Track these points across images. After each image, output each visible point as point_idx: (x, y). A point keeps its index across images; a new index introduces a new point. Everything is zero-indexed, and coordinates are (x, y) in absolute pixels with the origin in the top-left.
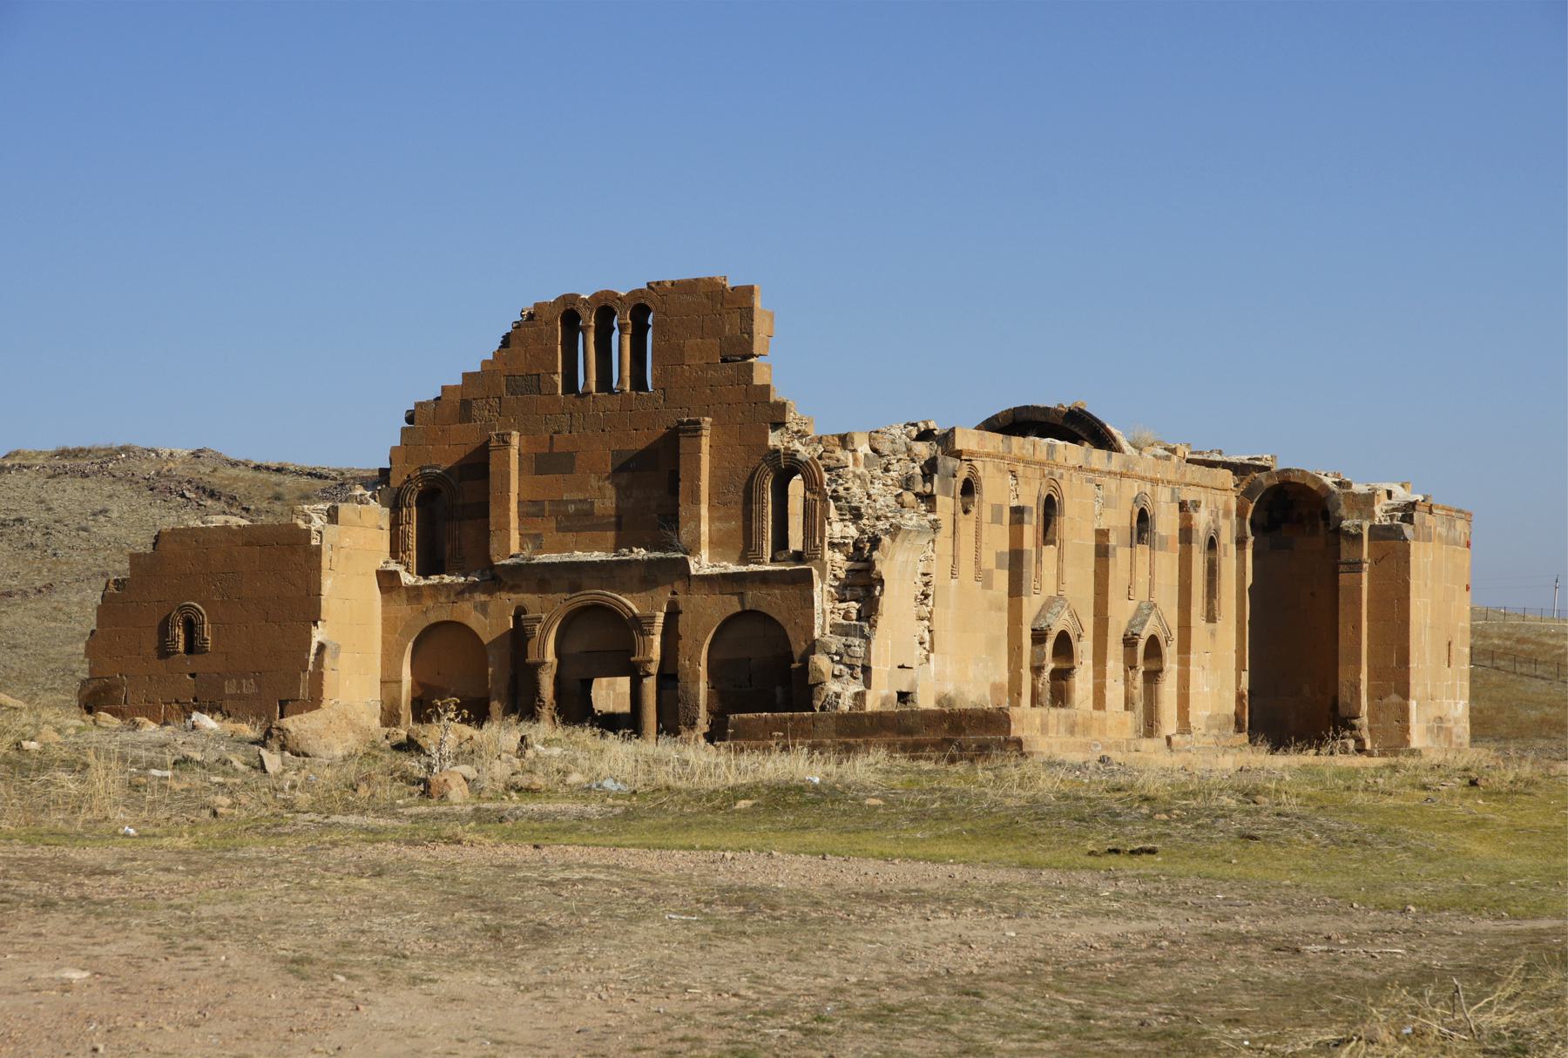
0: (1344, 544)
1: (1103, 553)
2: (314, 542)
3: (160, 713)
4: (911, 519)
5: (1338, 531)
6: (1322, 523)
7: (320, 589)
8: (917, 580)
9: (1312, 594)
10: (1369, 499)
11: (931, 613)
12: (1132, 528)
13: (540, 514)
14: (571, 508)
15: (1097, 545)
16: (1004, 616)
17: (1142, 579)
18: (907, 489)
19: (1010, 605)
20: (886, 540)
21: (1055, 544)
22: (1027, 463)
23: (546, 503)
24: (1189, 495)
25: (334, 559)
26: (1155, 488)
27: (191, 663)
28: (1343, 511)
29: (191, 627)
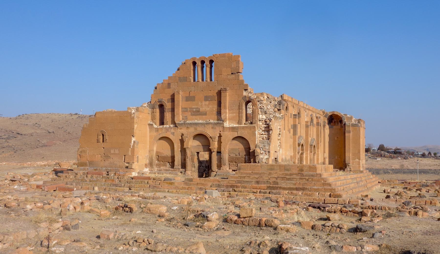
1: (307, 126)
2: (132, 116)
3: (96, 157)
4: (277, 115)
6: (339, 123)
7: (134, 128)
9: (337, 137)
11: (280, 138)
13: (187, 111)
14: (194, 110)
19: (293, 137)
20: (273, 119)
23: (188, 108)
24: (318, 115)
25: (137, 120)
27: (103, 145)
28: (346, 120)
29: (103, 135)
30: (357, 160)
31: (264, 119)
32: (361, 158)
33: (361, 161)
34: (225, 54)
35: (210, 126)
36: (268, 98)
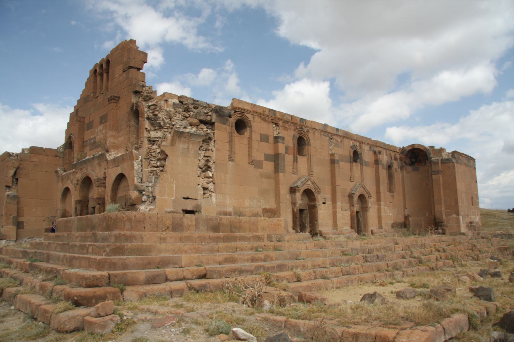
0: (433, 166)
1: (333, 162)
5: (431, 162)
8: (200, 158)
10: (441, 150)
12: (350, 156)
14: (92, 141)
15: (331, 160)
16: (272, 181)
17: (357, 174)
18: (196, 118)
21: (305, 155)
22: (285, 122)
24: (377, 149)
26: (362, 145)
28: (432, 155)
30: (454, 216)
31: (160, 138)
32: (461, 213)
33: (461, 217)
34: (119, 44)
35: (96, 162)
36: (181, 102)
